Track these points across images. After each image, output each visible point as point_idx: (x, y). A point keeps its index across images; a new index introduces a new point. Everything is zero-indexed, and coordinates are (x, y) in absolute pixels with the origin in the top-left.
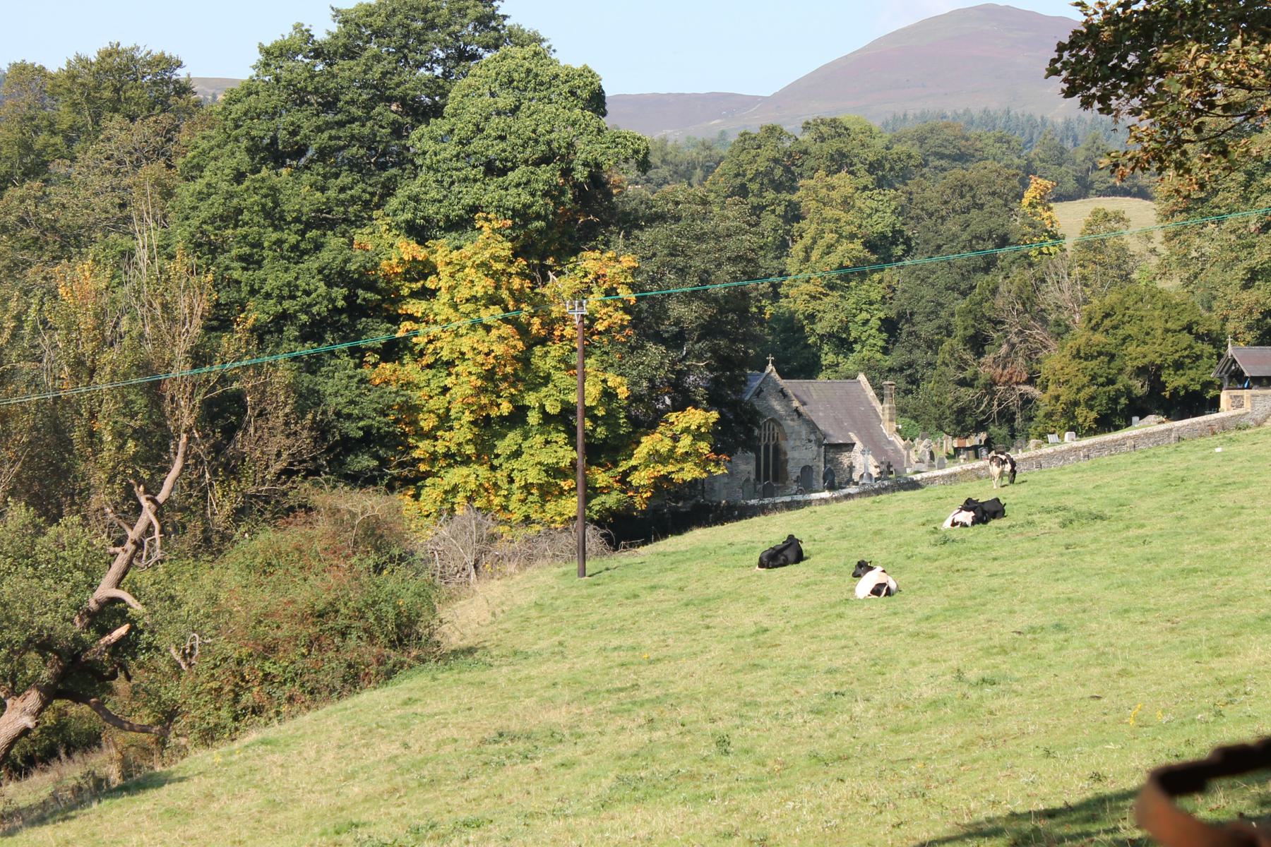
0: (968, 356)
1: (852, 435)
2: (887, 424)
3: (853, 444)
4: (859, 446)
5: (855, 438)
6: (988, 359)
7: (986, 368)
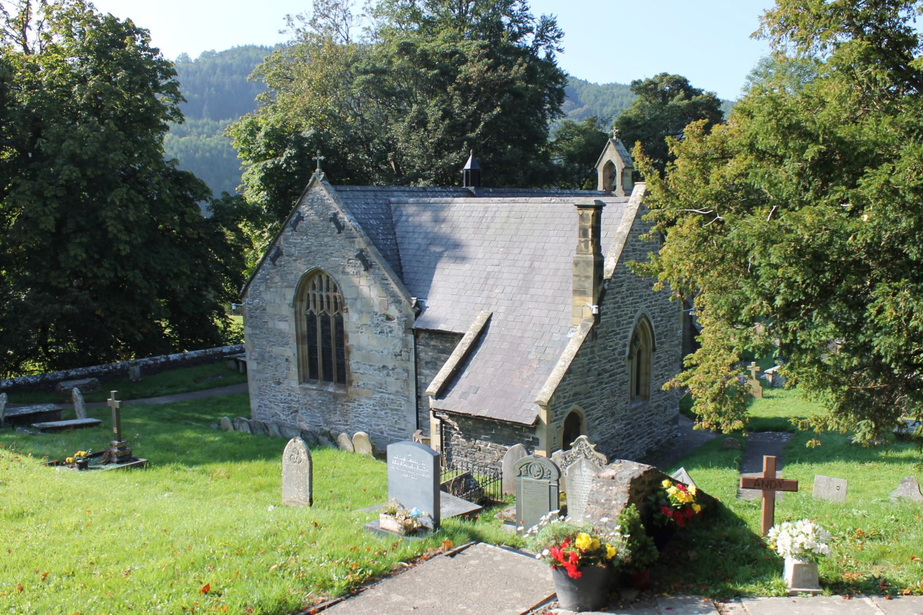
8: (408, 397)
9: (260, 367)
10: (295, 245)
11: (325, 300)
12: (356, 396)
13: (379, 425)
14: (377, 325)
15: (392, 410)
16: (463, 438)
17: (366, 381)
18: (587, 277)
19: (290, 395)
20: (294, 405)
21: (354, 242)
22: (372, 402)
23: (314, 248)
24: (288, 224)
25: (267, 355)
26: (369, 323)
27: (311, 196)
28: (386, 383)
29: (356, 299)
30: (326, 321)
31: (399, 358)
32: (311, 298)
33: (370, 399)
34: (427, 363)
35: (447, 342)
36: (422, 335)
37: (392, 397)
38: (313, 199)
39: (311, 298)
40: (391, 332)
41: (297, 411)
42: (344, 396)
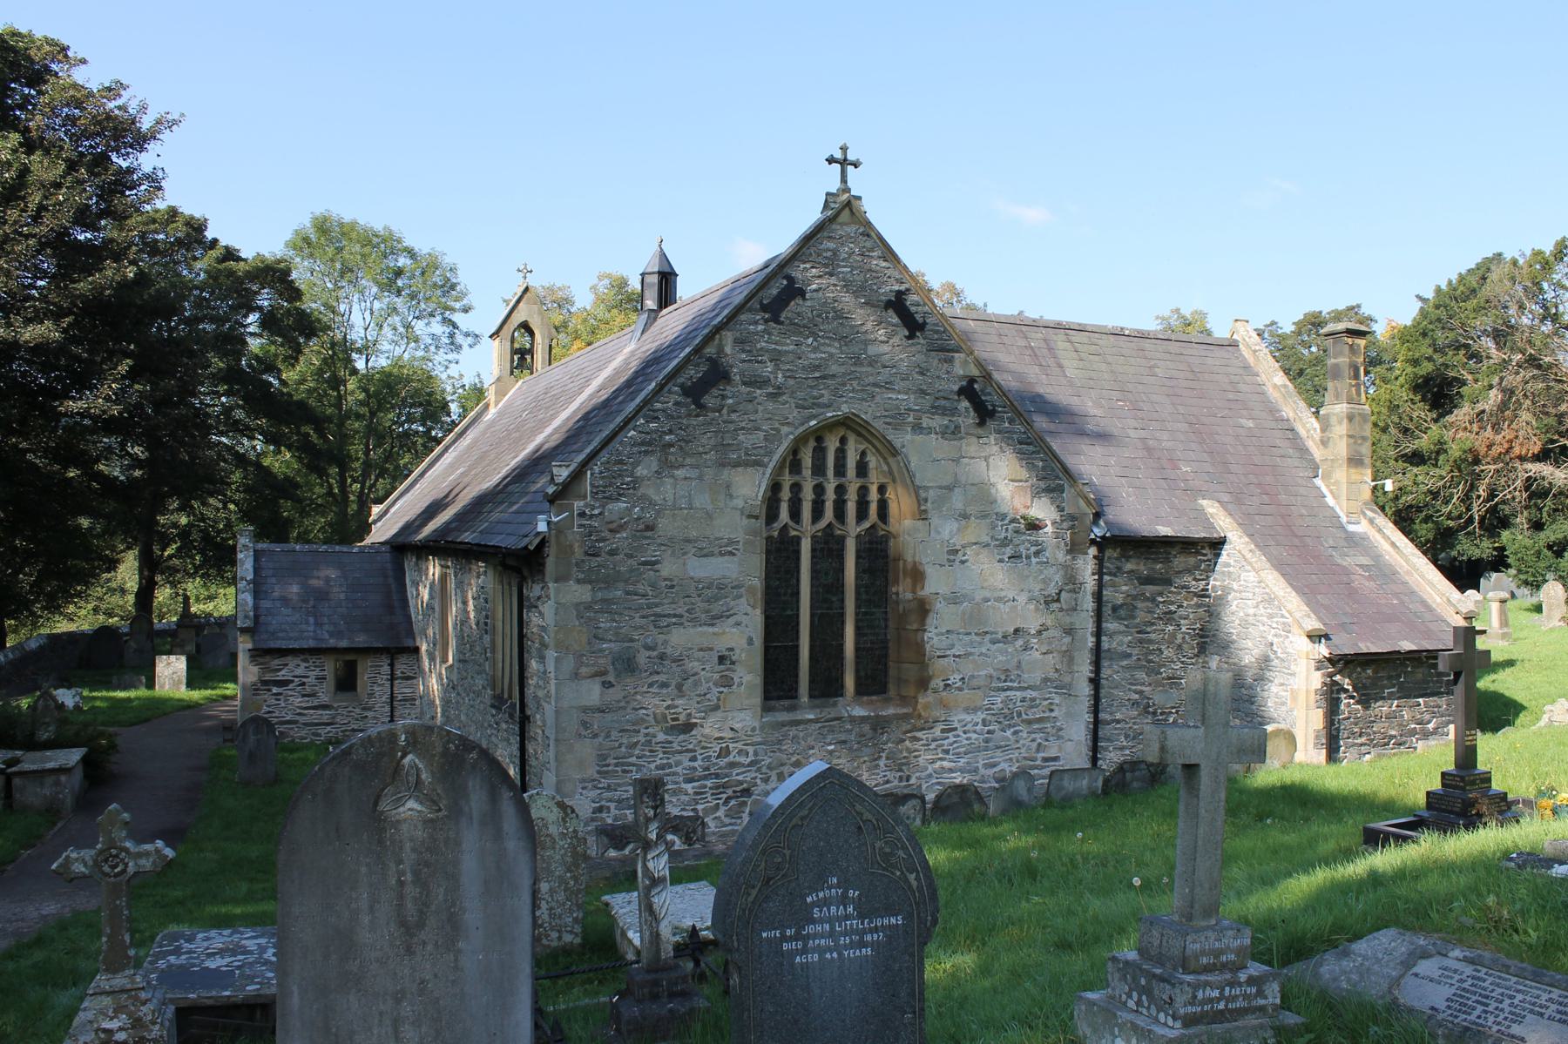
0: (1421, 412)
1: (1211, 507)
2: (1341, 474)
3: (1217, 544)
4: (1238, 545)
5: (1222, 522)
6: (1462, 414)
7: (1459, 431)
8: (1069, 686)
9: (615, 694)
10: (776, 358)
11: (830, 496)
12: (938, 713)
13: (994, 765)
14: (1005, 543)
15: (1029, 722)
16: (1358, 703)
17: (968, 669)
18: (1364, 438)
19: (724, 752)
20: (737, 775)
21: (950, 361)
22: (980, 716)
23: (834, 369)
24: (755, 304)
25: (642, 658)
26: (986, 539)
27: (831, 245)
28: (1019, 666)
29: (950, 488)
30: (828, 547)
31: (1055, 606)
32: (786, 494)
33: (975, 710)
34: (1115, 609)
35: (1156, 561)
36: (1109, 553)
37: (1029, 694)
38: (835, 252)
39: (786, 494)
40: (1037, 554)
41: (747, 792)
42: (905, 717)
